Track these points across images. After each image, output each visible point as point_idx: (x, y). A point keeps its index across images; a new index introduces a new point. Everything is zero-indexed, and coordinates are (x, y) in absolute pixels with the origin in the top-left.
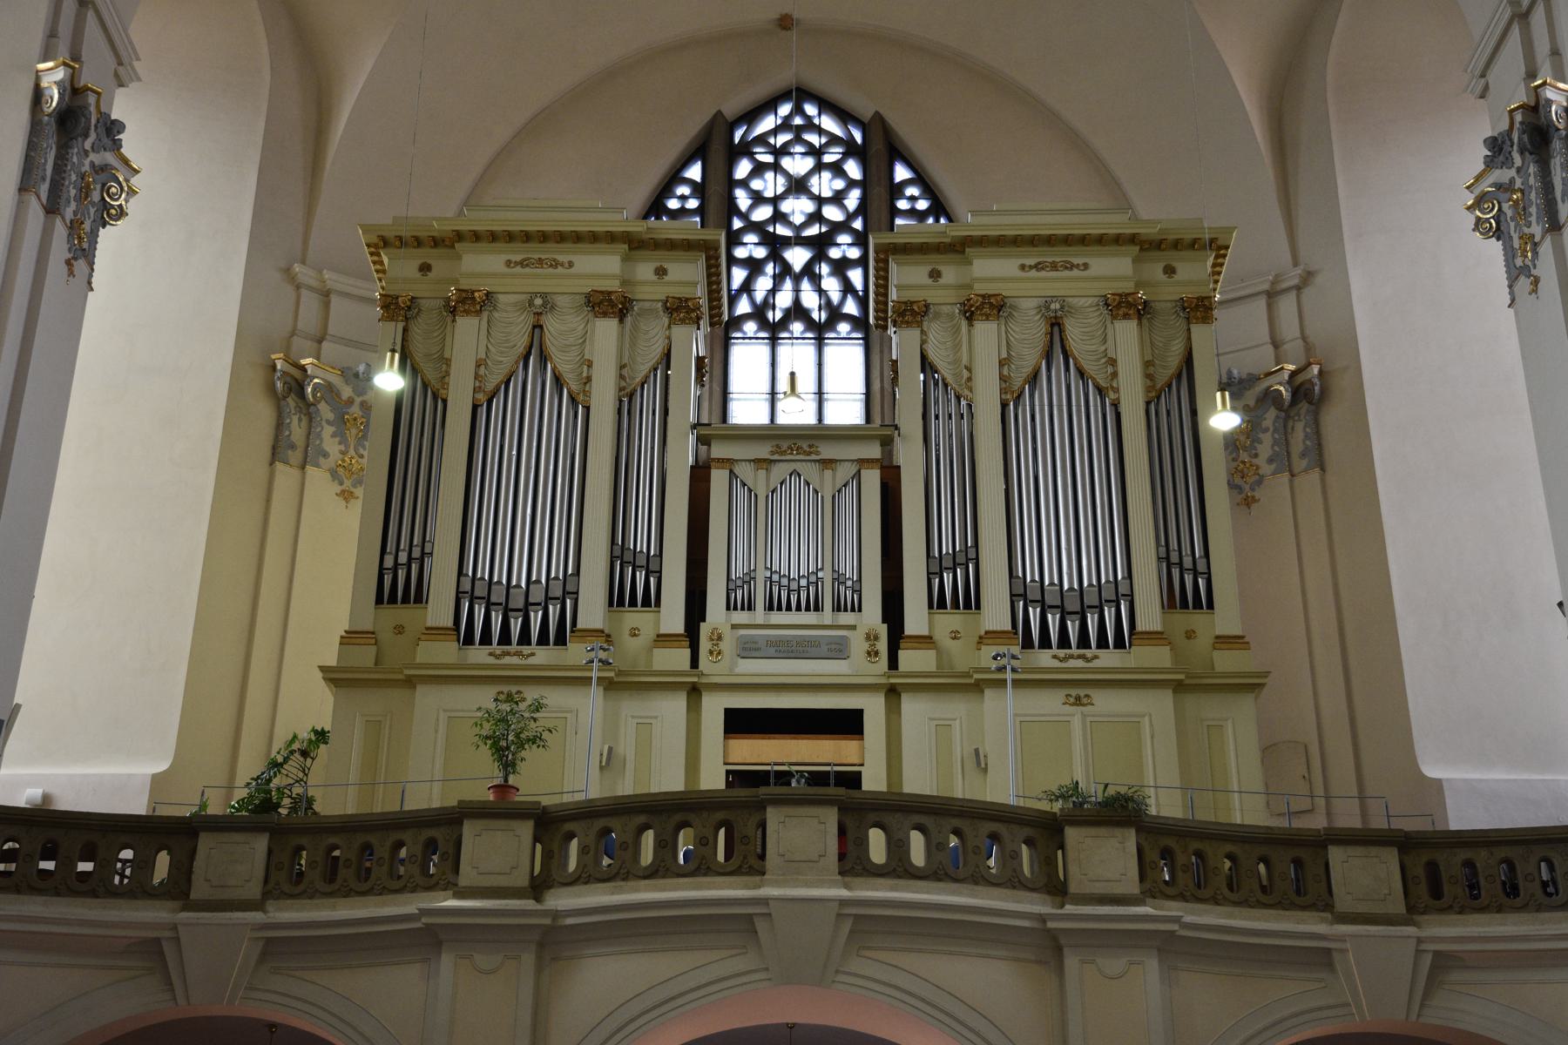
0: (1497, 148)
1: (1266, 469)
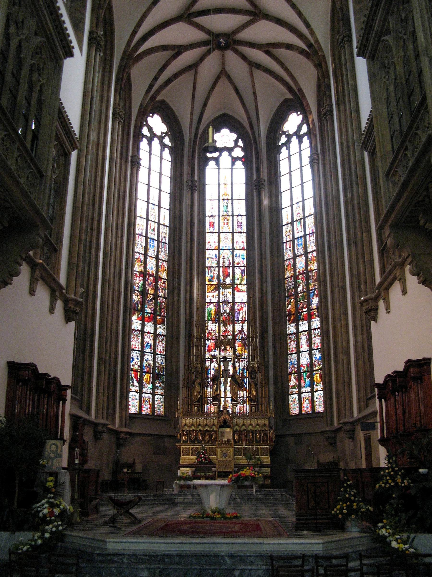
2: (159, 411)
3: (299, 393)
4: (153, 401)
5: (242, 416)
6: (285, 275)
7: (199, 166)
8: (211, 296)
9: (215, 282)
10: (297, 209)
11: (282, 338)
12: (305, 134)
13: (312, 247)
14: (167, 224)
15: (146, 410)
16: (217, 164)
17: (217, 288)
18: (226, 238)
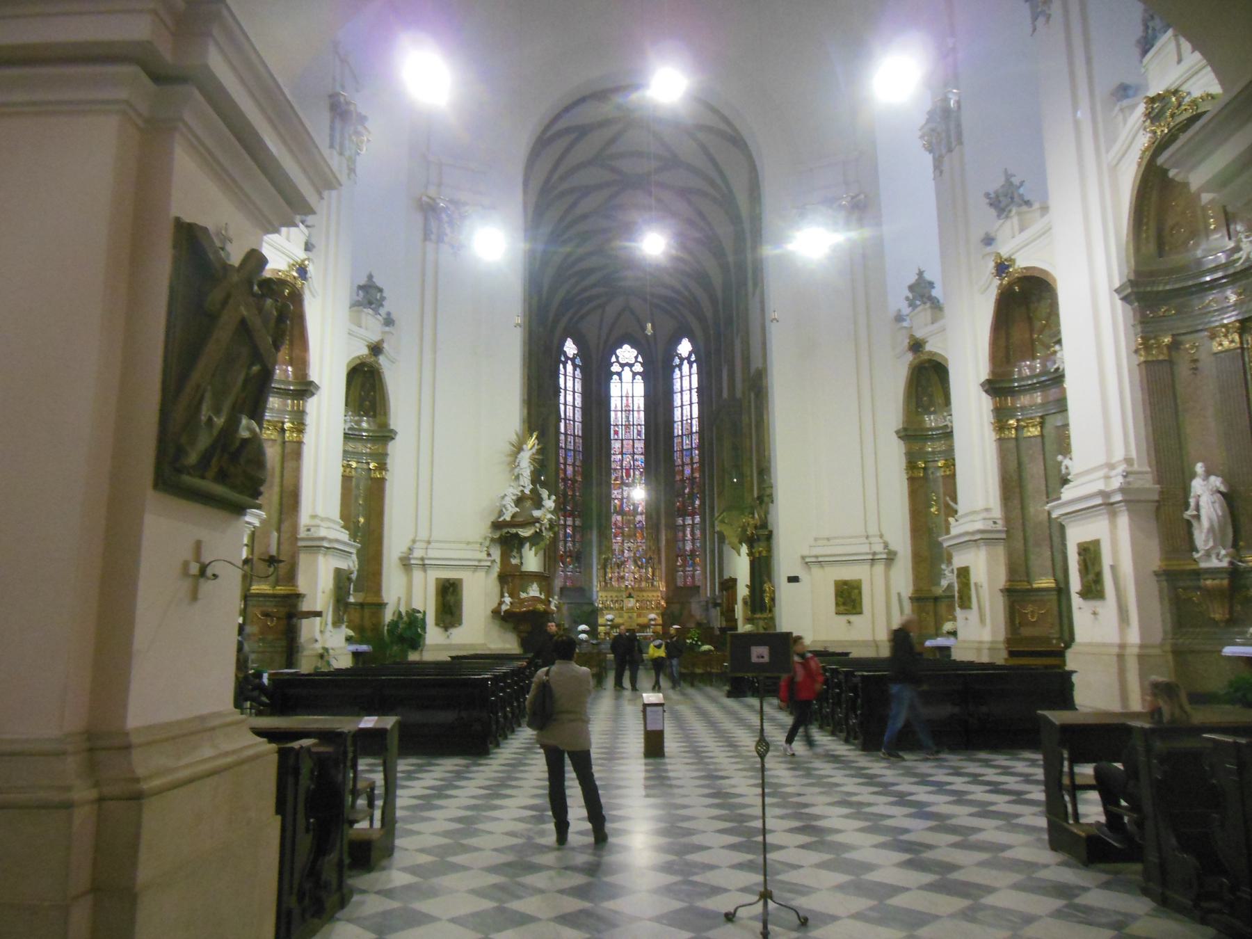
3: (684, 571)
13: (696, 459)
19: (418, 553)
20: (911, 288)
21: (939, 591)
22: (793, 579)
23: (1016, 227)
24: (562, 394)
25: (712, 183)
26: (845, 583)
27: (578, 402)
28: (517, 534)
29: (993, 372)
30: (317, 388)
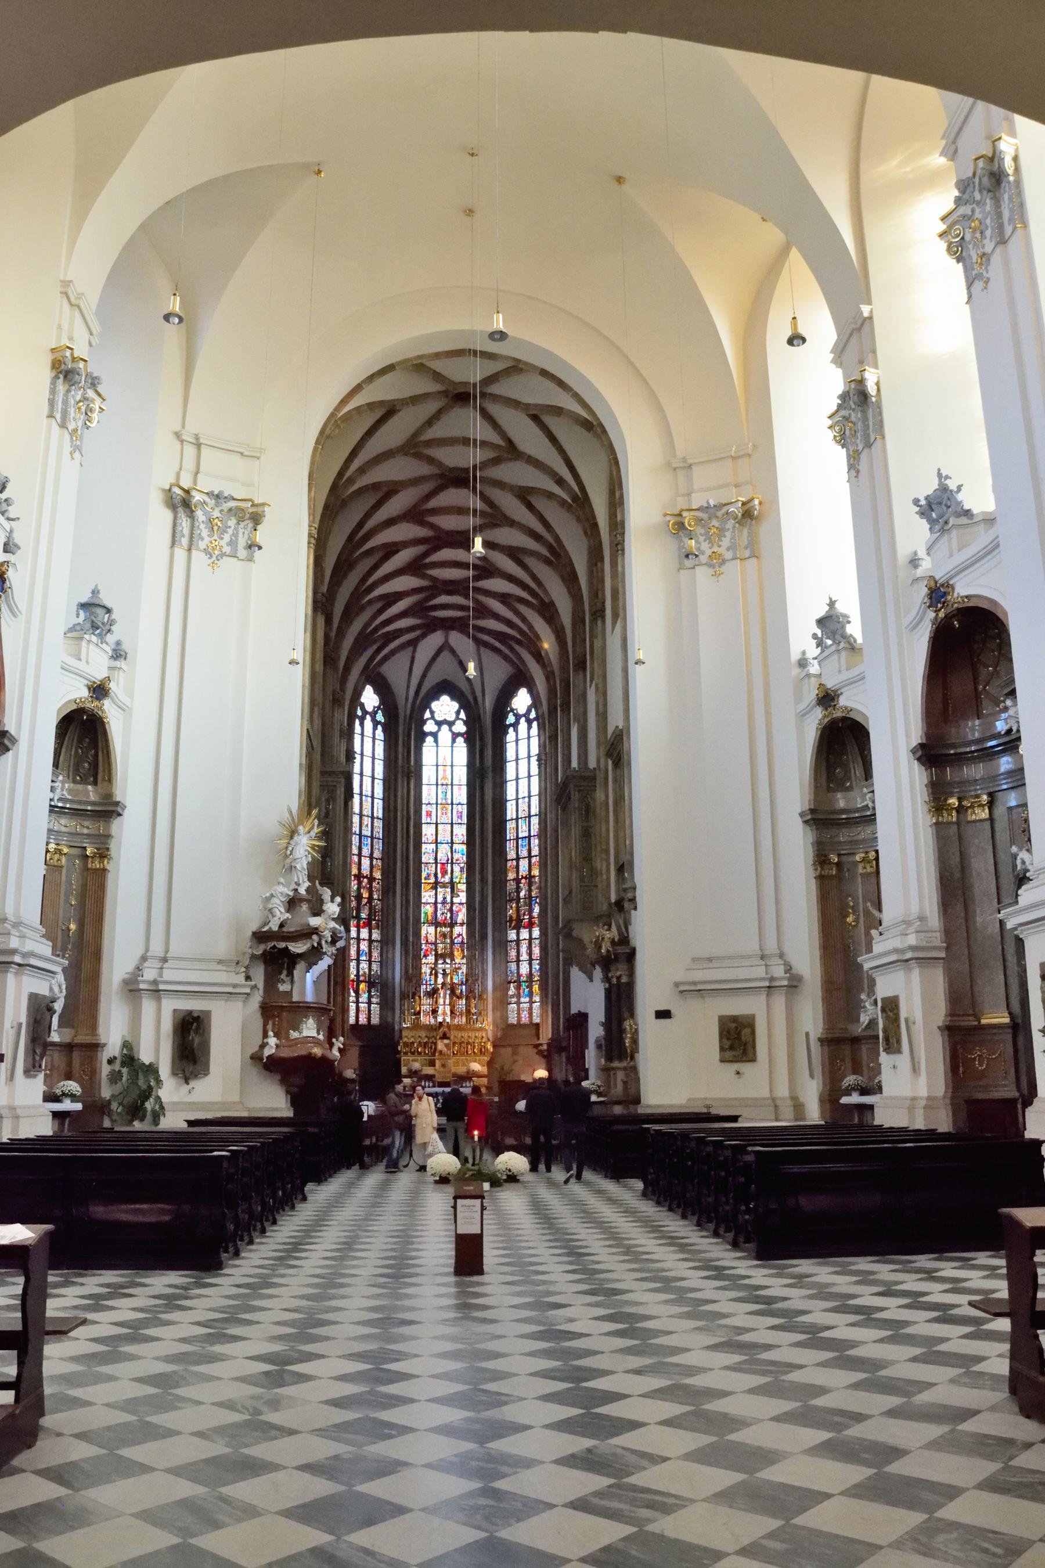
0: (844, 397)
1: (728, 555)
2: (375, 1020)
3: (518, 1003)
4: (369, 1010)
5: (459, 1028)
6: (506, 876)
7: (416, 747)
8: (427, 896)
9: (432, 880)
10: (523, 806)
11: (502, 945)
12: (535, 719)
13: (535, 851)
14: (381, 816)
15: (363, 1020)
16: (436, 741)
17: (435, 886)
18: (444, 830)
19: (149, 974)
20: (821, 622)
21: (858, 1030)
22: (663, 1014)
23: (955, 546)
24: (358, 761)
25: (560, 481)
26: (734, 1019)
27: (379, 772)
28: (287, 948)
29: (928, 735)
30: (14, 741)
